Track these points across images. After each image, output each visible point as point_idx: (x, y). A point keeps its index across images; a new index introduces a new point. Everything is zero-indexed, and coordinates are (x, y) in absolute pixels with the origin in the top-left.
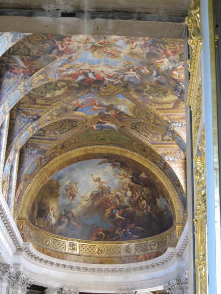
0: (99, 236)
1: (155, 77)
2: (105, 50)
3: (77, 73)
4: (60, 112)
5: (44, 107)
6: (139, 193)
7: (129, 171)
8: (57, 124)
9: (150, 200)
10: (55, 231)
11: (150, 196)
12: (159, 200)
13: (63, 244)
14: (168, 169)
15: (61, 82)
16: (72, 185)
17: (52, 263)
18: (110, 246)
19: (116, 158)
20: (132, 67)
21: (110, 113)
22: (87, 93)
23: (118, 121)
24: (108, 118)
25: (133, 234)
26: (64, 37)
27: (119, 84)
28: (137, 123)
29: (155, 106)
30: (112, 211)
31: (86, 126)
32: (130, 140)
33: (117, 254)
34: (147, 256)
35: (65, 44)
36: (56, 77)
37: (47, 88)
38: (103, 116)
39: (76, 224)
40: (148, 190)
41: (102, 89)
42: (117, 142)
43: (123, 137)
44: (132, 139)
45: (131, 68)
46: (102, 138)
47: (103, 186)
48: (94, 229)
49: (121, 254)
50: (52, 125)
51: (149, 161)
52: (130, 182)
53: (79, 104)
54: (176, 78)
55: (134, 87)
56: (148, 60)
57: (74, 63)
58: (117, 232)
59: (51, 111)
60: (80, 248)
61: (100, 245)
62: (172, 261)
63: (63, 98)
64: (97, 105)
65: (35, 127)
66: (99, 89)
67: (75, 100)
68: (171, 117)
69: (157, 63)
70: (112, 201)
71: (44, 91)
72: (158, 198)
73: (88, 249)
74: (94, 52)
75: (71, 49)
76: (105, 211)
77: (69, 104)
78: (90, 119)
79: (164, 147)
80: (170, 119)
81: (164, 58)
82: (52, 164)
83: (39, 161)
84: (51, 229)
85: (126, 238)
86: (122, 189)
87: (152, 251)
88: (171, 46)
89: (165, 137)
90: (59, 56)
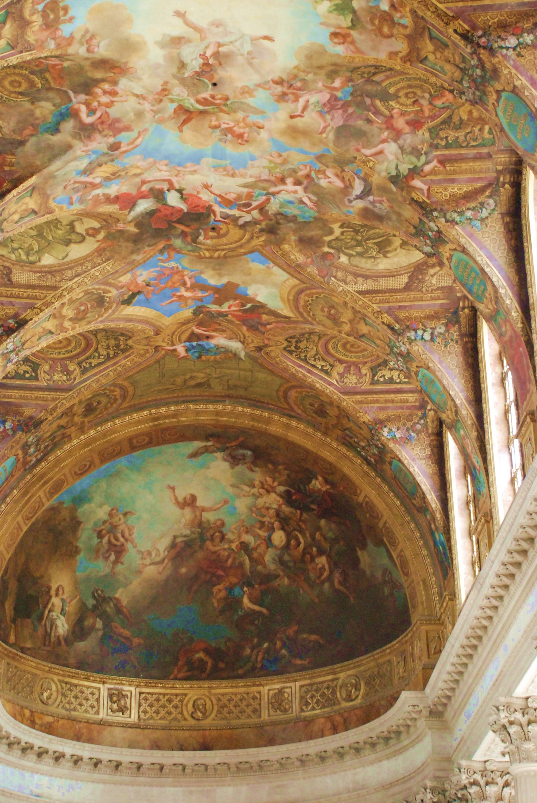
1: (358, 197)
2: (214, 123)
3: (134, 192)
4: (82, 308)
5: (36, 292)
6: (308, 535)
7: (277, 475)
8: (73, 345)
12: (365, 553)
13: (90, 696)
14: (390, 463)
15: (85, 220)
16: (116, 519)
17: (58, 757)
18: (226, 694)
19: (241, 439)
20: (294, 171)
21: (225, 308)
22: (161, 252)
23: (248, 330)
24: (220, 325)
26: (97, 82)
27: (255, 222)
28: (303, 335)
29: (356, 283)
30: (230, 589)
31: (157, 348)
32: (281, 386)
33: (249, 716)
34: (338, 718)
35: (99, 102)
36: (71, 204)
37: (44, 238)
38: (205, 318)
40: (333, 526)
41: (206, 238)
42: (242, 393)
43: (262, 376)
44: (288, 381)
45: (290, 176)
46: (199, 381)
47: (203, 519)
48: (180, 644)
49: (260, 716)
50: (57, 346)
51: (334, 444)
52: (280, 506)
53: (137, 284)
54: (420, 200)
55: (295, 231)
56: (339, 150)
57: (127, 161)
58: (248, 651)
59: (57, 304)
60: (140, 705)
63: (93, 267)
64: (189, 284)
65: (12, 351)
66: (195, 240)
67: (128, 272)
68: (402, 315)
69: (366, 156)
70: (230, 561)
71: (36, 247)
72: (364, 547)
73: (164, 706)
74: (185, 128)
75: (118, 120)
76: (212, 593)
77: (110, 285)
78: (167, 327)
79: (377, 401)
80: (397, 320)
81: (385, 141)
82: (59, 461)
83: (20, 452)
84: (55, 652)
86: (258, 525)
87: (351, 704)
88: (407, 106)
89: (379, 374)
90: (80, 139)
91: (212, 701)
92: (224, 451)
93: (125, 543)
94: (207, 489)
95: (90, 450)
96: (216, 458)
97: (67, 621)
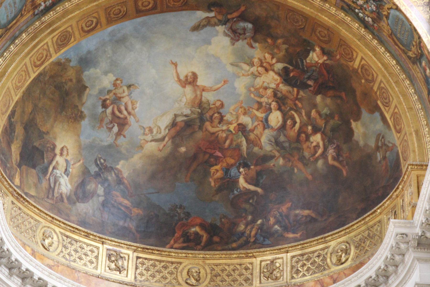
0: (192, 237)
6: (304, 114)
7: (275, 51)
9: (333, 130)
10: (68, 215)
11: (333, 118)
12: (359, 123)
13: (89, 253)
16: (121, 90)
18: (220, 264)
19: (243, 8)
25: (286, 229)
30: (227, 171)
39: (126, 202)
40: (328, 101)
47: (203, 99)
48: (177, 218)
51: (333, 10)
52: (278, 85)
58: (242, 227)
60: (136, 268)
61: (192, 261)
62: (402, 271)
70: (228, 142)
72: (357, 117)
76: (210, 172)
82: (66, 13)
84: (58, 207)
85: (267, 242)
86: (256, 106)
91: (206, 271)
92: (225, 24)
93: (128, 118)
94: (208, 66)
95: (97, 5)
96: (217, 32)
97: (71, 181)
